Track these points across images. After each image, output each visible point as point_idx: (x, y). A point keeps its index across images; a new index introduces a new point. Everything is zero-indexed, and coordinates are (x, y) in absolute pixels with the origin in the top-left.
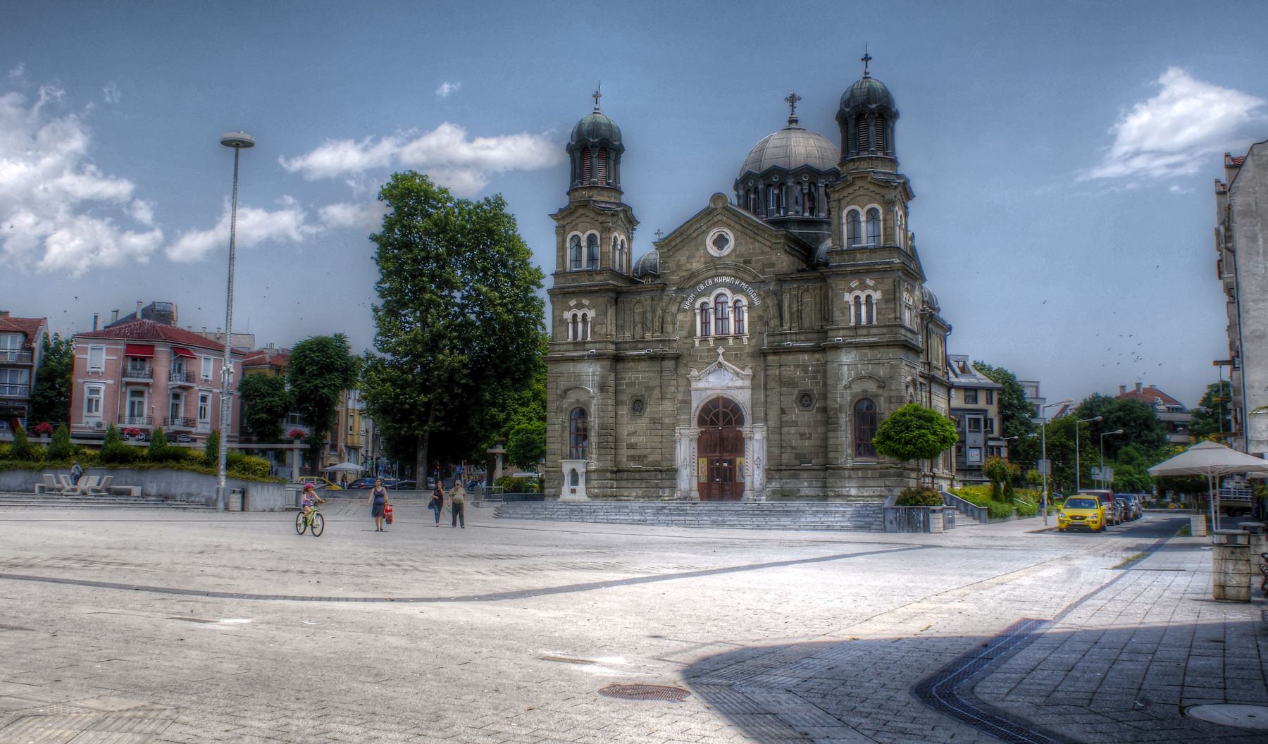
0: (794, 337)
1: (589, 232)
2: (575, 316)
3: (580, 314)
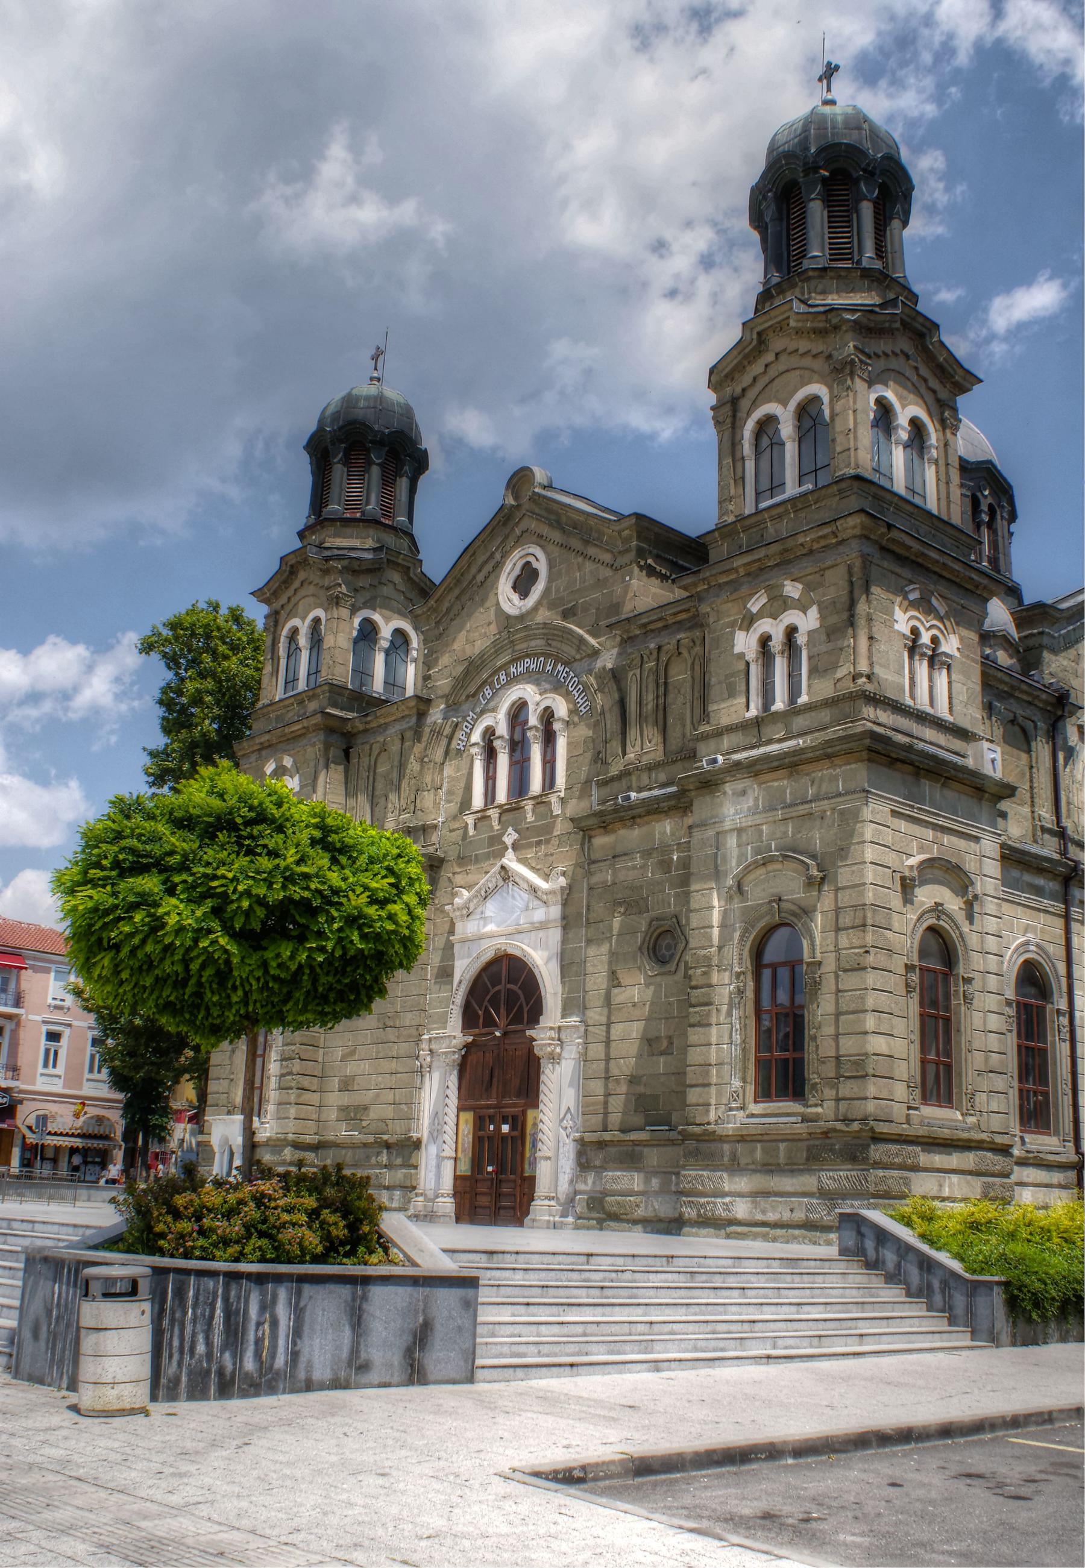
1: (311, 616)
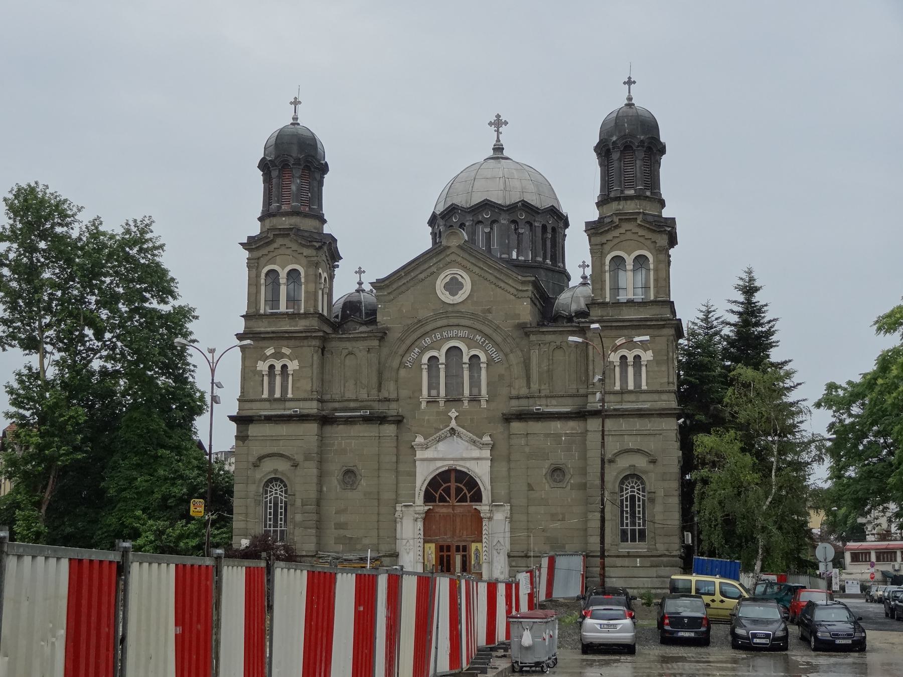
0: (543, 401)
2: (272, 367)
3: (278, 367)
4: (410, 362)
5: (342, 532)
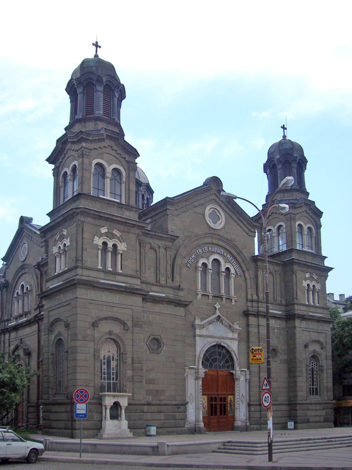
3: (110, 245)
4: (190, 264)
5: (151, 387)
